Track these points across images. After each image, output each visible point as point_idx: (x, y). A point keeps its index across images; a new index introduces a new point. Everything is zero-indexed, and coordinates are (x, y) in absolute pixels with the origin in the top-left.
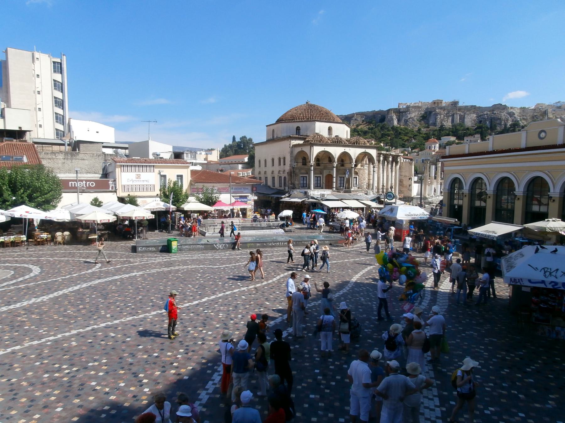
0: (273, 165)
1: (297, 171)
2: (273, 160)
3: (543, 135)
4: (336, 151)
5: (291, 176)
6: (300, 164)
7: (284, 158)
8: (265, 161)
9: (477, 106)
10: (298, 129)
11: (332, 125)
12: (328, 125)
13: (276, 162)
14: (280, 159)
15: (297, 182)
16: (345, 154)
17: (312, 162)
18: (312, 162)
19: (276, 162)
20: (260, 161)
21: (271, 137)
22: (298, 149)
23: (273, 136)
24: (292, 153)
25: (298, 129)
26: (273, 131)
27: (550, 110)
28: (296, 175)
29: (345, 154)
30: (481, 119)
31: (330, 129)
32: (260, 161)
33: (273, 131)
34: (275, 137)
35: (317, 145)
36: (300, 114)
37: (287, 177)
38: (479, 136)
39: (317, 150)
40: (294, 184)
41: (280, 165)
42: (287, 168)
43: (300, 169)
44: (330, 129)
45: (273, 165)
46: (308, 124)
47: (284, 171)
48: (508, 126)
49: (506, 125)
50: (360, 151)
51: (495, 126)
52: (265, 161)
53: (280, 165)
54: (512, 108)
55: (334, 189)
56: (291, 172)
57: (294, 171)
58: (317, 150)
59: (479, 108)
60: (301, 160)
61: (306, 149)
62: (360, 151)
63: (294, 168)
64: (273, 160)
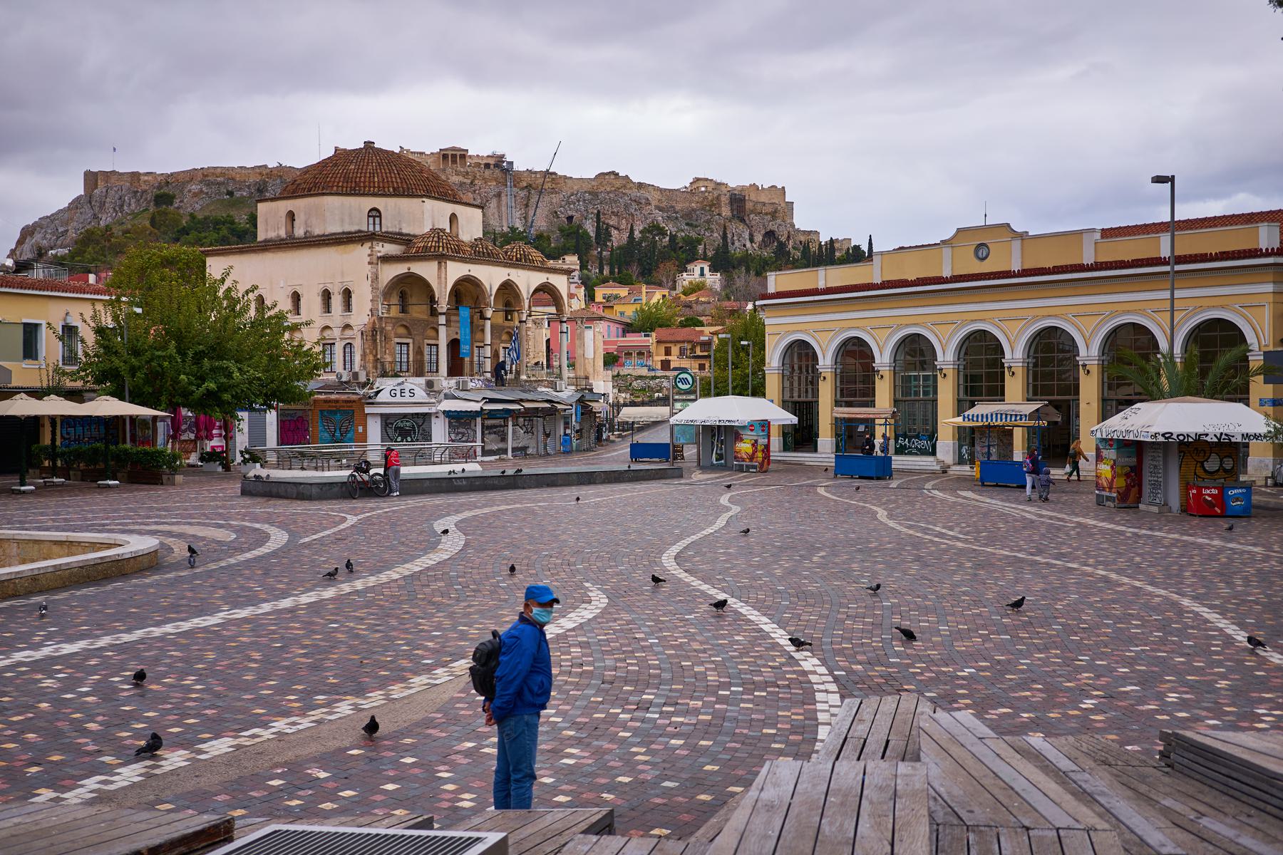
2: (296, 298)
3: (982, 253)
4: (491, 277)
5: (375, 341)
6: (395, 312)
7: (347, 294)
10: (375, 213)
11: (459, 210)
12: (449, 208)
13: (311, 305)
14: (327, 296)
15: (388, 358)
16: (508, 289)
17: (443, 306)
18: (443, 306)
19: (311, 305)
22: (401, 269)
23: (291, 235)
24: (375, 278)
25: (375, 213)
26: (291, 216)
28: (387, 339)
29: (508, 289)
30: (570, 213)
31: (453, 218)
33: (291, 216)
34: (299, 232)
35: (453, 259)
36: (372, 175)
37: (358, 344)
38: (575, 259)
39: (456, 271)
40: (383, 364)
42: (361, 316)
44: (453, 218)
46: (404, 203)
47: (347, 327)
48: (637, 234)
50: (538, 278)
54: (641, 185)
55: (489, 375)
56: (374, 330)
57: (382, 330)
58: (456, 271)
60: (395, 300)
61: (426, 270)
62: (538, 278)
64: (296, 298)
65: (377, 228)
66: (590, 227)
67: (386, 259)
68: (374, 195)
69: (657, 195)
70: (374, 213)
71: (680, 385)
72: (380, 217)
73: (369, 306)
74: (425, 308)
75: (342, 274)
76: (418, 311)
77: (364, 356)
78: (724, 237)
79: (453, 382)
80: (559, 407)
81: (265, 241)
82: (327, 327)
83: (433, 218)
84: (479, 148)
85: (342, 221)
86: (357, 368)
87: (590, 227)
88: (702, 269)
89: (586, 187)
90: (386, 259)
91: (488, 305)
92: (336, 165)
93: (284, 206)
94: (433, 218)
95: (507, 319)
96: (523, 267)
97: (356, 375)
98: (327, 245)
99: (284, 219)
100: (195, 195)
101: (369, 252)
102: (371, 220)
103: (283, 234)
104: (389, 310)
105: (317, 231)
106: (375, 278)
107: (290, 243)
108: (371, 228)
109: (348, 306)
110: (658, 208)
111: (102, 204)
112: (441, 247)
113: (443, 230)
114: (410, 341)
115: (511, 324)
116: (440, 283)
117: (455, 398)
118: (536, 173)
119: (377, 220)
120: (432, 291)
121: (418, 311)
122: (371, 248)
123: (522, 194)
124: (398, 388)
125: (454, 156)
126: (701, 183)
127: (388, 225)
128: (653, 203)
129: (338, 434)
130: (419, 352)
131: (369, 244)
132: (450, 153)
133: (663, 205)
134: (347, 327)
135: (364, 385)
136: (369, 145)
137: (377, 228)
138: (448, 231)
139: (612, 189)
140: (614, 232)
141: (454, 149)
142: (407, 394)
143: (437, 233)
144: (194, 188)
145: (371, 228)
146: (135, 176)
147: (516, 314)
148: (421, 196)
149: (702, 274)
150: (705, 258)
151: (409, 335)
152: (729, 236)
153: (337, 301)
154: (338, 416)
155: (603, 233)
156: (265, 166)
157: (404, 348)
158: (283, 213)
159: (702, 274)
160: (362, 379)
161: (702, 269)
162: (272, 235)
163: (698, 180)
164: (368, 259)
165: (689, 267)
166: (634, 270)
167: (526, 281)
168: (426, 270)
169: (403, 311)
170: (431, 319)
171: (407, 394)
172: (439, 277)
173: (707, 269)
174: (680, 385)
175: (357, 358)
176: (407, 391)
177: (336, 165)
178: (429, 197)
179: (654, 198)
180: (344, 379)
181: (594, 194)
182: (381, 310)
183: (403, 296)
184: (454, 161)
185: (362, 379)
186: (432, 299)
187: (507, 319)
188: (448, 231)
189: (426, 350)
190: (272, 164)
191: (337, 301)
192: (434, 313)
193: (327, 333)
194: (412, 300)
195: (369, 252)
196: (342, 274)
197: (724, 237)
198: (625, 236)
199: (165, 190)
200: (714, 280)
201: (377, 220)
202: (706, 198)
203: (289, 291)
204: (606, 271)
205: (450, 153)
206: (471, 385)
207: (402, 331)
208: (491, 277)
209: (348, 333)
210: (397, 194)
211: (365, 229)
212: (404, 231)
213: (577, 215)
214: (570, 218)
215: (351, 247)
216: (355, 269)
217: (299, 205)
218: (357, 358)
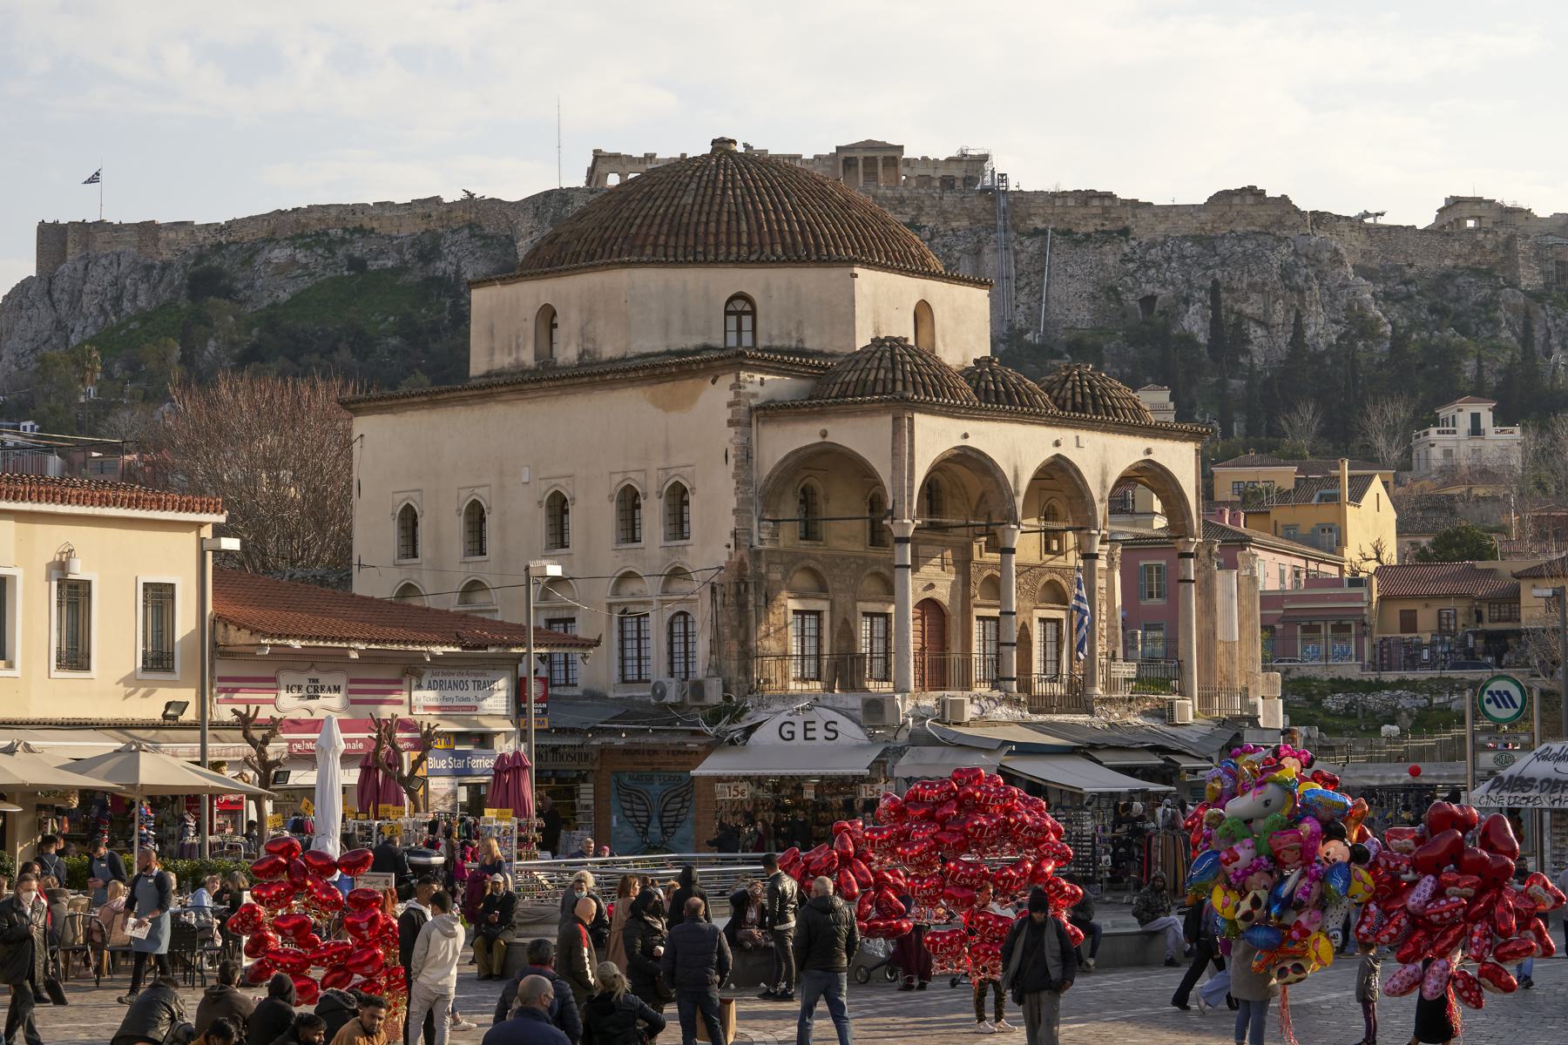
0: (558, 537)
1: (776, 576)
2: (558, 507)
5: (742, 606)
6: (789, 536)
7: (678, 497)
8: (476, 516)
9: (1123, 194)
10: (741, 307)
12: (911, 289)
13: (594, 516)
14: (629, 502)
16: (1057, 473)
19: (594, 516)
20: (409, 520)
21: (528, 357)
24: (746, 457)
25: (741, 307)
26: (548, 318)
27: (1521, 246)
30: (1149, 289)
31: (923, 313)
32: (409, 520)
33: (548, 318)
34: (567, 352)
37: (702, 613)
38: (1163, 396)
39: (935, 436)
41: (629, 529)
43: (791, 562)
44: (923, 313)
45: (558, 537)
46: (809, 279)
47: (677, 573)
49: (1299, 329)
51: (1241, 341)
52: (476, 516)
53: (629, 529)
57: (760, 579)
58: (935, 436)
59: (1135, 203)
61: (863, 435)
63: (758, 553)
64: (558, 507)
65: (747, 340)
66: (1194, 322)
67: (771, 411)
68: (740, 262)
69: (1358, 242)
70: (740, 305)
71: (1491, 708)
72: (753, 313)
73: (730, 523)
74: (860, 528)
75: (667, 448)
76: (845, 535)
77: (716, 643)
78: (1526, 339)
79: (929, 701)
80: (1185, 763)
81: (488, 375)
82: (629, 576)
83: (876, 313)
84: (927, 141)
85: (666, 325)
86: (700, 669)
87: (1194, 322)
88: (1476, 418)
89: (1188, 226)
90: (771, 411)
91: (1011, 517)
92: (649, 196)
93: (531, 294)
94: (876, 313)
95: (1048, 550)
96: (1092, 426)
97: (698, 689)
98: (632, 382)
99: (530, 326)
100: (280, 270)
101: (730, 396)
102: (733, 320)
103: (528, 357)
104: (775, 535)
105: (609, 350)
106: (746, 457)
107: (544, 378)
108: (732, 342)
109: (678, 525)
110: (1360, 270)
111: (76, 298)
112: (899, 378)
113: (900, 342)
114: (822, 605)
115: (1060, 561)
116: (896, 467)
117: (932, 741)
118: (1064, 195)
119: (747, 321)
120: (879, 483)
121: (845, 535)
122: (737, 386)
123: (1031, 246)
124: (799, 721)
125: (870, 163)
126: (1466, 207)
127: (772, 331)
128: (1348, 261)
129: (655, 829)
130: (846, 633)
131: (727, 380)
132: (860, 155)
133: (1375, 263)
134: (677, 573)
135: (715, 716)
136: (722, 145)
137: (747, 340)
138: (911, 342)
139: (1248, 223)
140: (1256, 333)
141: (870, 145)
142: (820, 733)
143: (885, 347)
144: (280, 254)
145: (732, 342)
146: (148, 230)
147: (1071, 539)
148: (852, 262)
149: (1476, 430)
150: (1479, 393)
151: (822, 589)
152: (1539, 335)
153: (653, 515)
154: (656, 788)
155: (1228, 338)
156: (436, 200)
157: (811, 622)
158: (530, 312)
159: (1476, 430)
160: (714, 696)
161: (1476, 418)
162: (503, 361)
163: (1454, 203)
164: (728, 414)
165: (1443, 413)
166: (1305, 420)
167: (1102, 456)
168: (863, 435)
169: (809, 533)
170: (874, 553)
171: (820, 733)
172: (896, 453)
173: (1487, 419)
174: (1491, 708)
175: (702, 646)
176: (820, 726)
177: (649, 196)
178: (870, 265)
179: (1350, 247)
180: (672, 697)
181: (1205, 241)
182: (761, 536)
183: (807, 499)
184: (871, 175)
185: (714, 696)
186: (876, 508)
187: (1048, 550)
188: (911, 342)
189: (864, 628)
190: (451, 195)
191: (653, 515)
192: (878, 536)
193: (633, 586)
194: (832, 508)
195: (730, 396)
196: (667, 448)
197: (1526, 339)
198: (1283, 340)
199: (216, 261)
200: (1504, 444)
201: (747, 321)
202: (1477, 246)
203: (544, 491)
204: (1237, 428)
205: (860, 155)
206: (971, 711)
207: (801, 580)
208: (1018, 447)
209: (677, 585)
210: (794, 257)
211: (718, 341)
212: (810, 345)
213: (1164, 294)
214: (1148, 301)
215: (687, 385)
216: (696, 435)
217: (568, 291)
218: (702, 646)
